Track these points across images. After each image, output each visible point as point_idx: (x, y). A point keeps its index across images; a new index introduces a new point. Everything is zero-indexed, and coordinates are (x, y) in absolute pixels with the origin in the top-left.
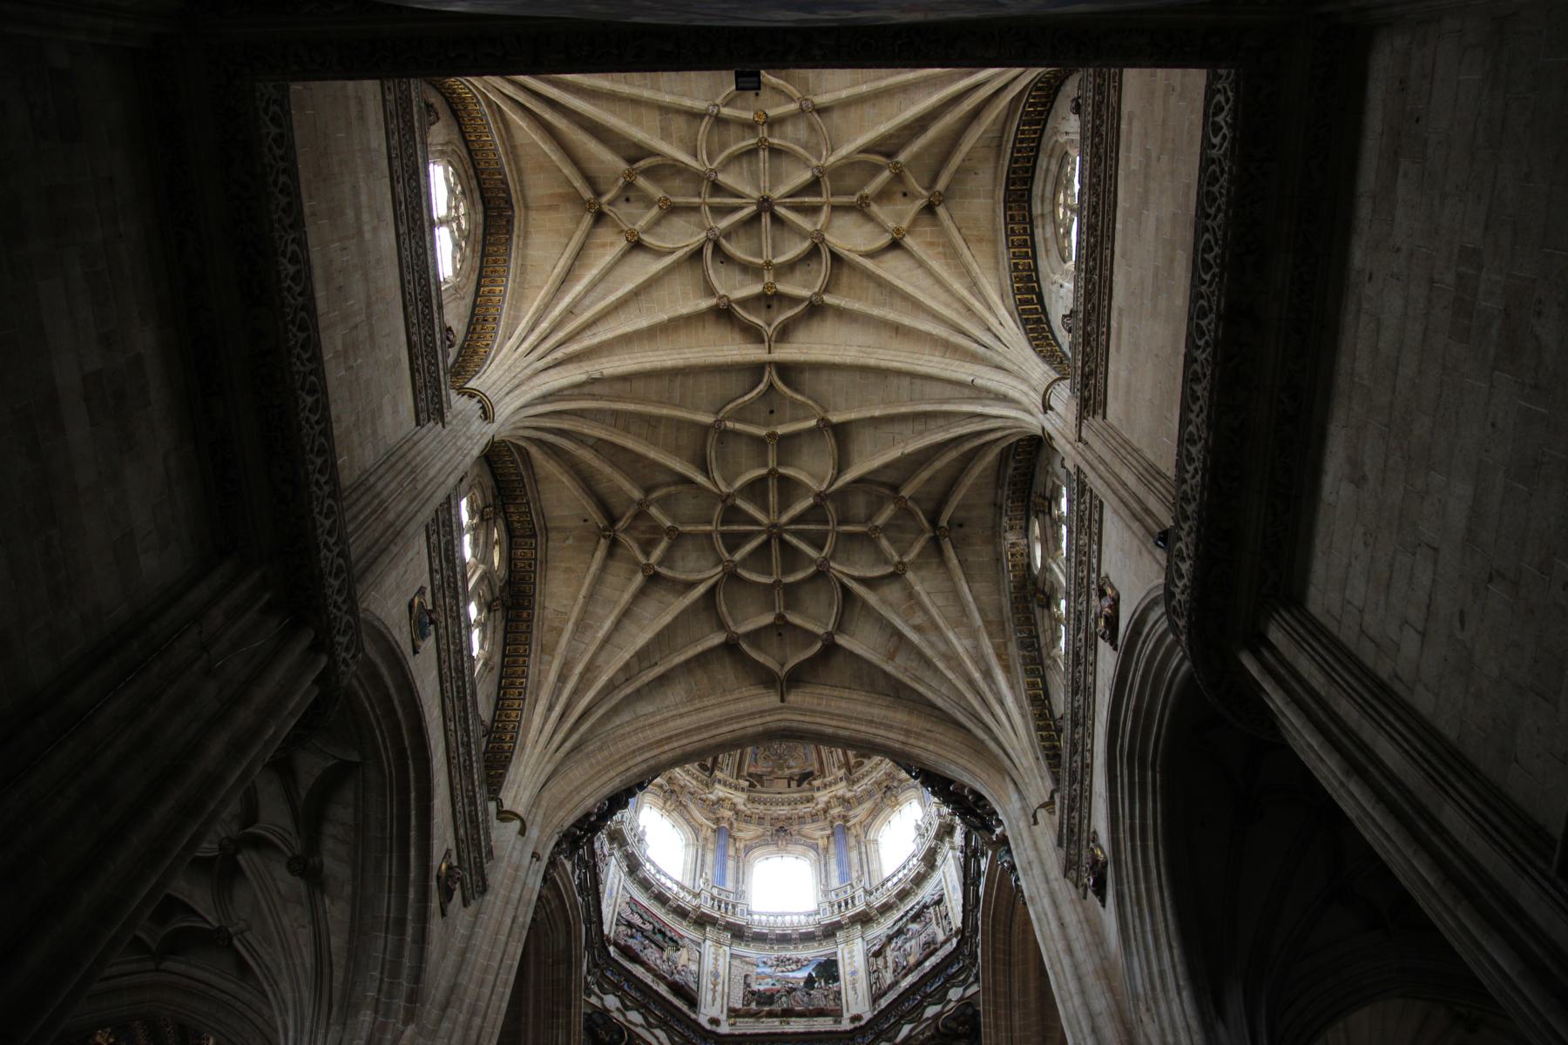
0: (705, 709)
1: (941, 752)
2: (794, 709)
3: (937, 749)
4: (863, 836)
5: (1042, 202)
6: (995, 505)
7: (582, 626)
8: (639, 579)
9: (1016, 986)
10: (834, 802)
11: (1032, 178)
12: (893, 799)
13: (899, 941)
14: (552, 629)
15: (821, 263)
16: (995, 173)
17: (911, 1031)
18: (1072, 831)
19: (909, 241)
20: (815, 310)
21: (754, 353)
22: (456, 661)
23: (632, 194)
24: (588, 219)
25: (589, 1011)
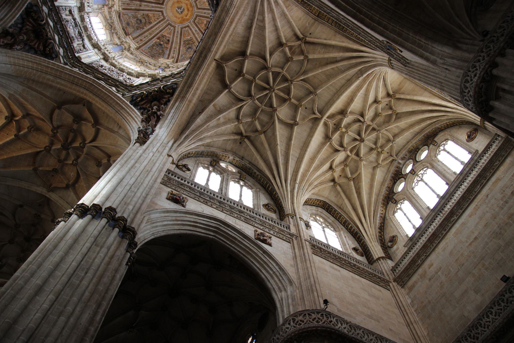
0: (230, 36)
1: (182, 112)
2: (211, 63)
3: (182, 111)
4: (100, 11)
5: (321, 212)
6: (243, 157)
7: (284, 15)
8: (284, 41)
9: (63, 82)
10: (113, 3)
11: (327, 211)
12: (108, 28)
13: (73, 24)
14: (289, 5)
15: (337, 145)
16: (332, 202)
18: (182, 185)
19: (330, 173)
20: (327, 138)
21: (328, 114)
22: (358, 32)
23: (387, 107)
24: (391, 93)
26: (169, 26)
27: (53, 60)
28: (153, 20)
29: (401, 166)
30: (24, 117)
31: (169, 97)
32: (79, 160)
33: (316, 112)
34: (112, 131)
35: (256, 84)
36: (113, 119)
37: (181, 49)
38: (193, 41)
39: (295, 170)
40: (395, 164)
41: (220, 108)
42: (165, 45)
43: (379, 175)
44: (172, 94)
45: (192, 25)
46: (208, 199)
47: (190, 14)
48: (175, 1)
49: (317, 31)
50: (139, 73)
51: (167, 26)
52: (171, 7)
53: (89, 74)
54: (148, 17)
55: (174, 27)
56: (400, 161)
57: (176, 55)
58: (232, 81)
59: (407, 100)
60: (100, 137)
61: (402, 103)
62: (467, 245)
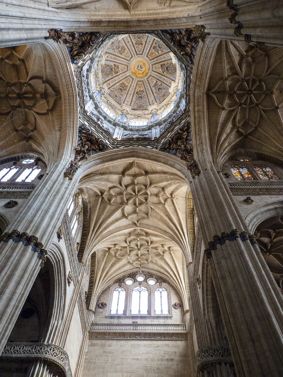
2: (131, 160)
20: (130, 234)
23: (163, 250)
26: (126, 67)
27: (72, 64)
29: (138, 273)
30: (20, 60)
31: (97, 149)
32: (18, 109)
33: (139, 223)
34: (54, 128)
36: (61, 121)
37: (117, 84)
39: (103, 236)
40: (138, 269)
43: (128, 267)
44: (101, 150)
45: (135, 81)
46: (68, 239)
47: (141, 75)
49: (181, 201)
50: (93, 96)
51: (125, 65)
53: (78, 87)
56: (140, 271)
57: (111, 85)
58: (129, 175)
59: (172, 257)
60: (44, 117)
61: (170, 256)
62: (132, 357)
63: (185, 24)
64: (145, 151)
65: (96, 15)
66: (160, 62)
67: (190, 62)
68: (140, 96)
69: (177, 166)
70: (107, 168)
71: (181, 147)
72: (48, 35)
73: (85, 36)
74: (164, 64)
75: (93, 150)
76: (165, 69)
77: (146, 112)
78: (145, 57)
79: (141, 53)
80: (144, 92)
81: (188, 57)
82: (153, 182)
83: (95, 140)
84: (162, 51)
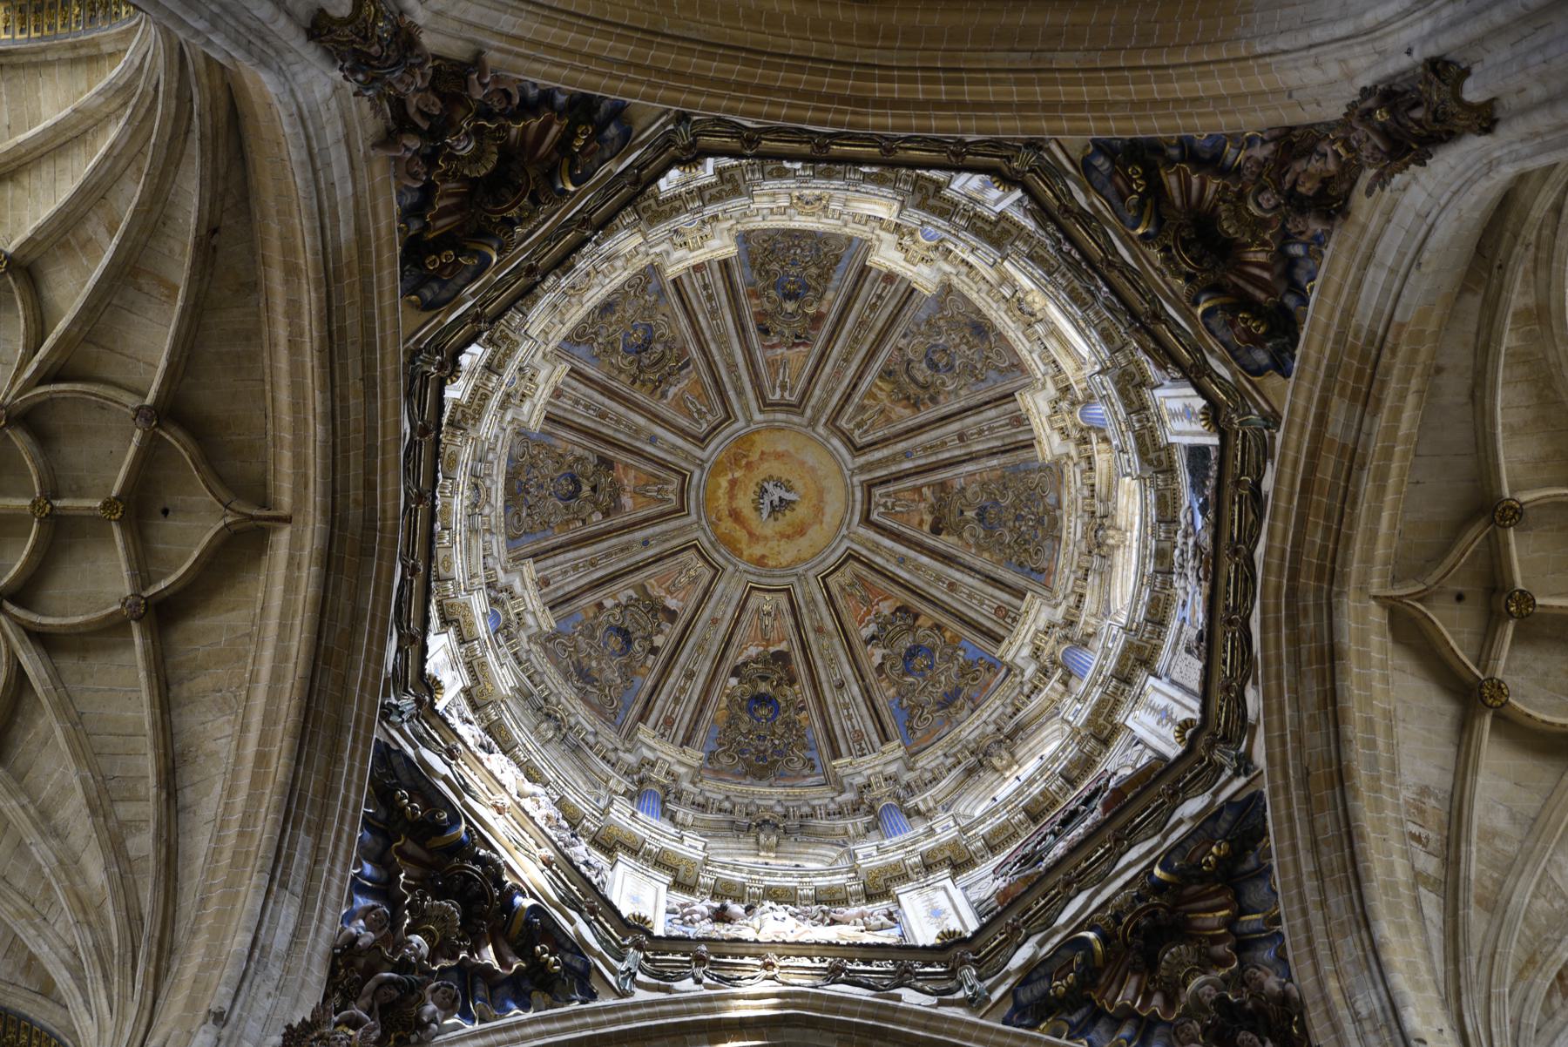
0: (254, 678)
17: (1168, 299)
25: (1007, 1007)
26: (794, 399)
28: (882, 395)
31: (426, 227)
35: (27, 493)
37: (683, 322)
38: (643, 383)
41: (140, 290)
42: (768, 307)
44: (414, 251)
45: (688, 456)
47: (723, 502)
48: (817, 527)
51: (806, 394)
52: (821, 492)
54: (908, 398)
55: (766, 405)
58: (150, 460)
63: (1337, 997)
64: (373, 616)
65: (1406, 379)
66: (804, 647)
67: (1025, 996)
68: (586, 489)
69: (288, 912)
70: (251, 286)
71: (411, 930)
72: (1473, 92)
73: (1278, 269)
74: (792, 681)
75: (428, 191)
76: (764, 687)
77: (498, 544)
78: (846, 544)
79: (874, 517)
80: (606, 514)
81: (1069, 986)
82: (68, 663)
83: (496, 218)
84: (880, 669)
